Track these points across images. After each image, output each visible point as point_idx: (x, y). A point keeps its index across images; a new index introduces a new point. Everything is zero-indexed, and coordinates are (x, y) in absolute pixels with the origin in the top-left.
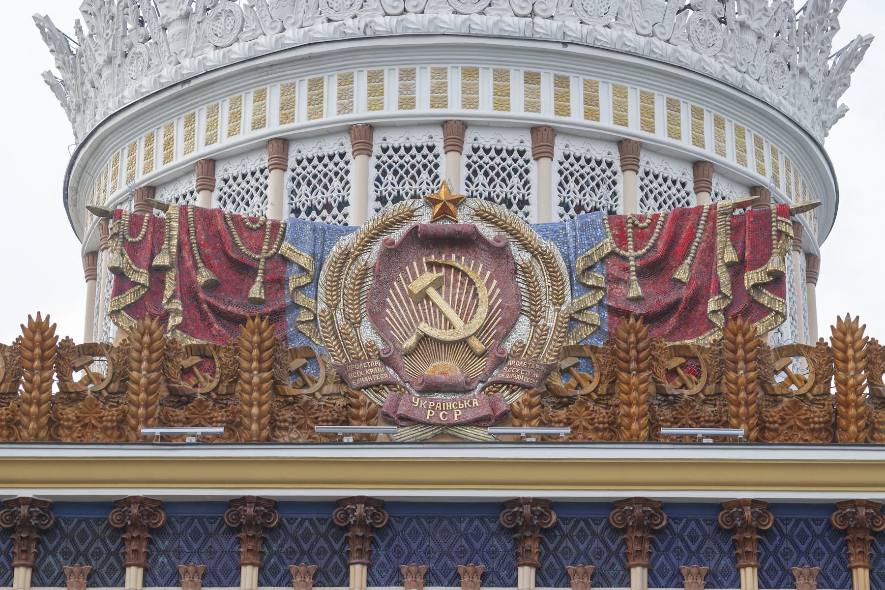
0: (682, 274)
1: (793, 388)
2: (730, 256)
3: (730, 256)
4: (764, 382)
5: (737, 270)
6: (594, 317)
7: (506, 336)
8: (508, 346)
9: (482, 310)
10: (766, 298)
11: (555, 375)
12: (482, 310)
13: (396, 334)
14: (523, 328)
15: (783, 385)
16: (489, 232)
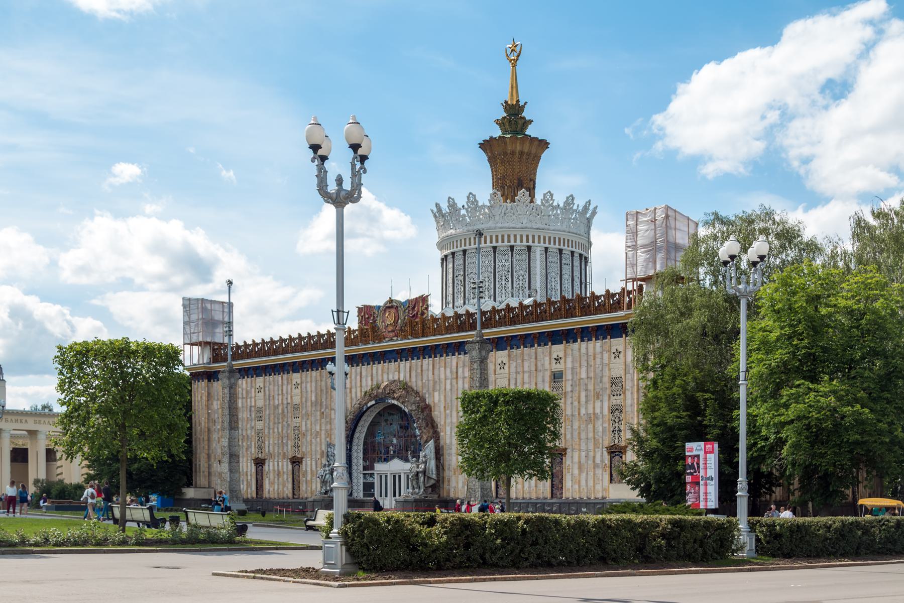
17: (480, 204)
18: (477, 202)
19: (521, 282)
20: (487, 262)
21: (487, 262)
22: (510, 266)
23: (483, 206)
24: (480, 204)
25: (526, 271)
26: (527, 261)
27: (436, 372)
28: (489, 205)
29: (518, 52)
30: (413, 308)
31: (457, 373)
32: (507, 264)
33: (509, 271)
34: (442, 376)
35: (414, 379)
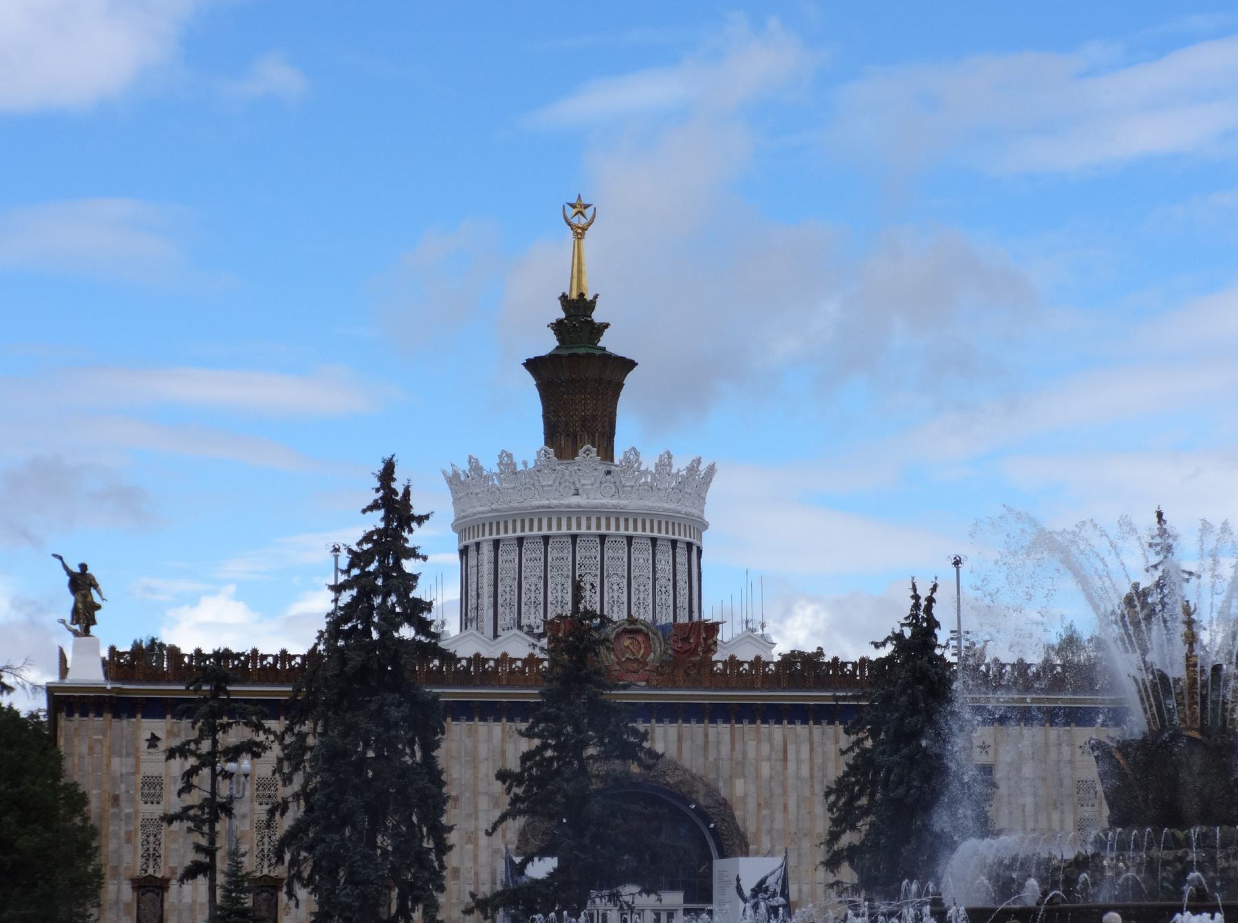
0: (692, 641)
1: (718, 671)
2: (704, 635)
3: (704, 635)
4: (711, 671)
5: (706, 639)
6: (670, 652)
7: (647, 658)
8: (648, 660)
9: (642, 651)
10: (713, 647)
11: (660, 668)
12: (642, 651)
13: (620, 656)
14: (652, 655)
15: (716, 671)
16: (643, 628)
17: (643, 468)
18: (640, 464)
19: (615, 595)
20: (641, 561)
21: (641, 561)
22: (671, 570)
23: (646, 472)
24: (643, 468)
25: (568, 576)
26: (687, 565)
27: (738, 746)
28: (654, 471)
29: (589, 219)
30: (685, 640)
31: (785, 751)
32: (667, 568)
33: (669, 580)
34: (751, 754)
35: (686, 754)
